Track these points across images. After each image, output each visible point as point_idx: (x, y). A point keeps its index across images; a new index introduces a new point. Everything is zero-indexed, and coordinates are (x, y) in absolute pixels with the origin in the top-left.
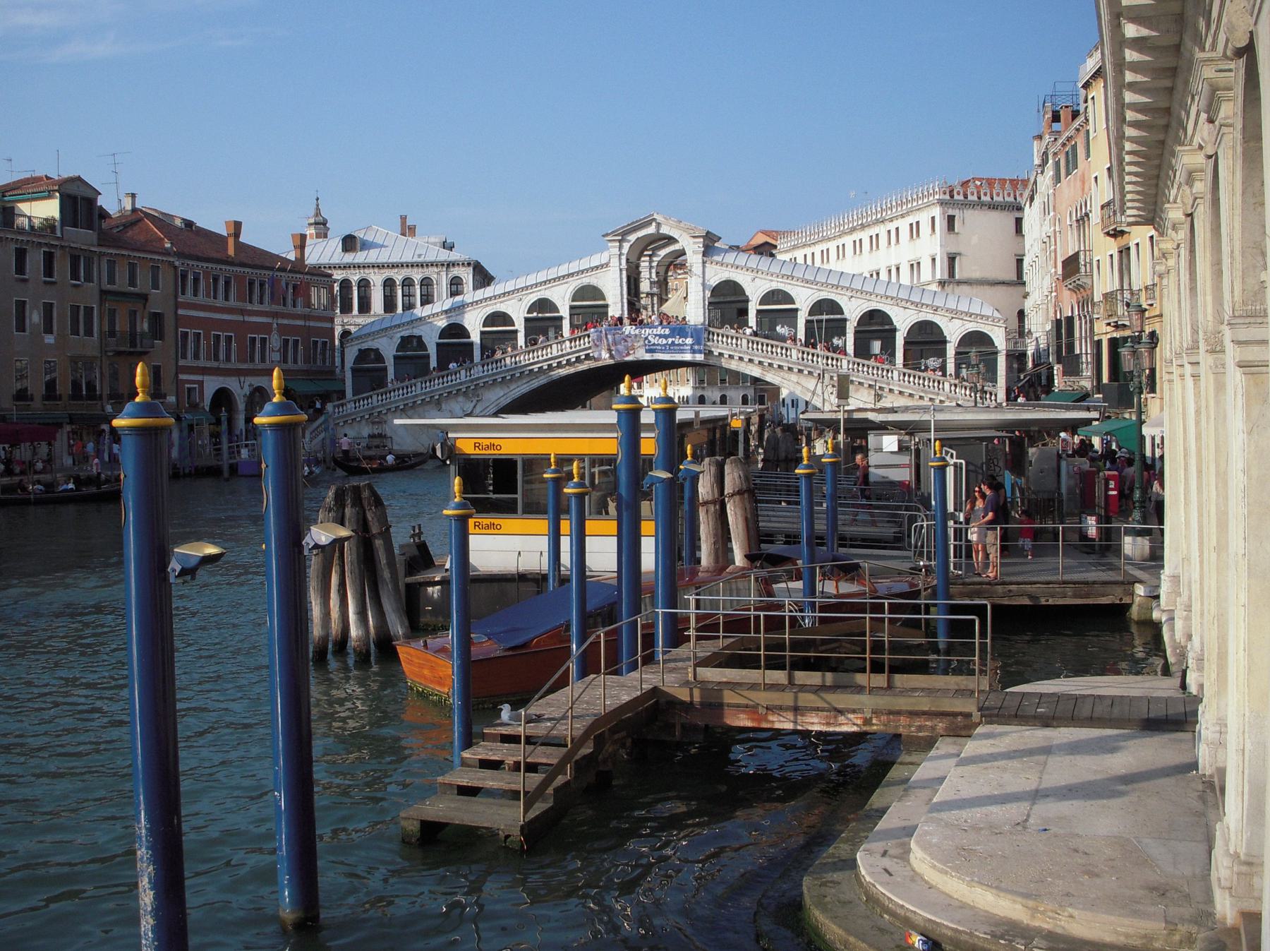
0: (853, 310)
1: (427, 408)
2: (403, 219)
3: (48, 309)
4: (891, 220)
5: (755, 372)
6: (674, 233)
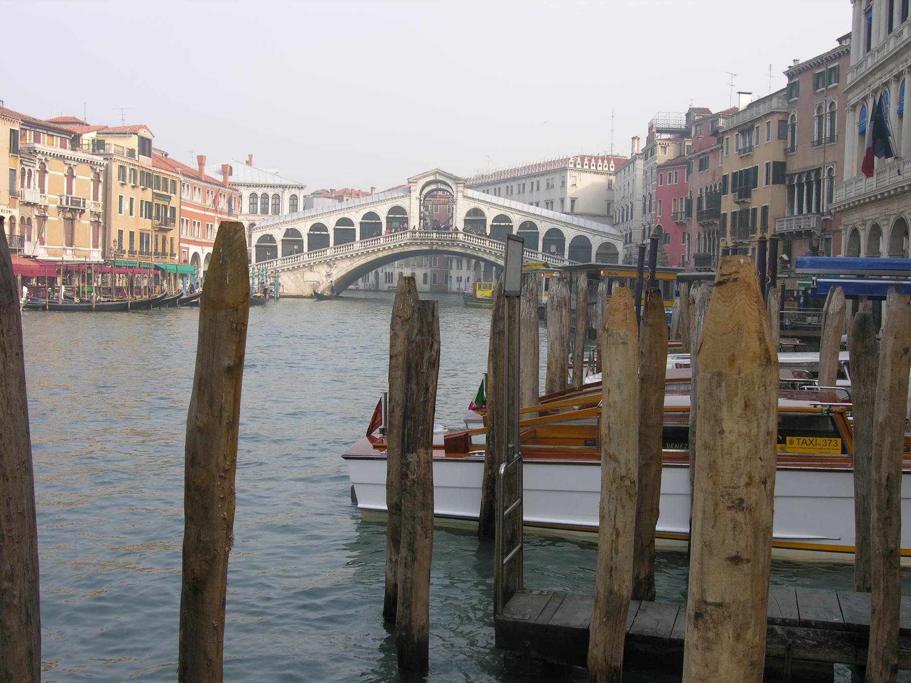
0: (543, 228)
2: (251, 156)
3: (132, 199)
4: (534, 176)
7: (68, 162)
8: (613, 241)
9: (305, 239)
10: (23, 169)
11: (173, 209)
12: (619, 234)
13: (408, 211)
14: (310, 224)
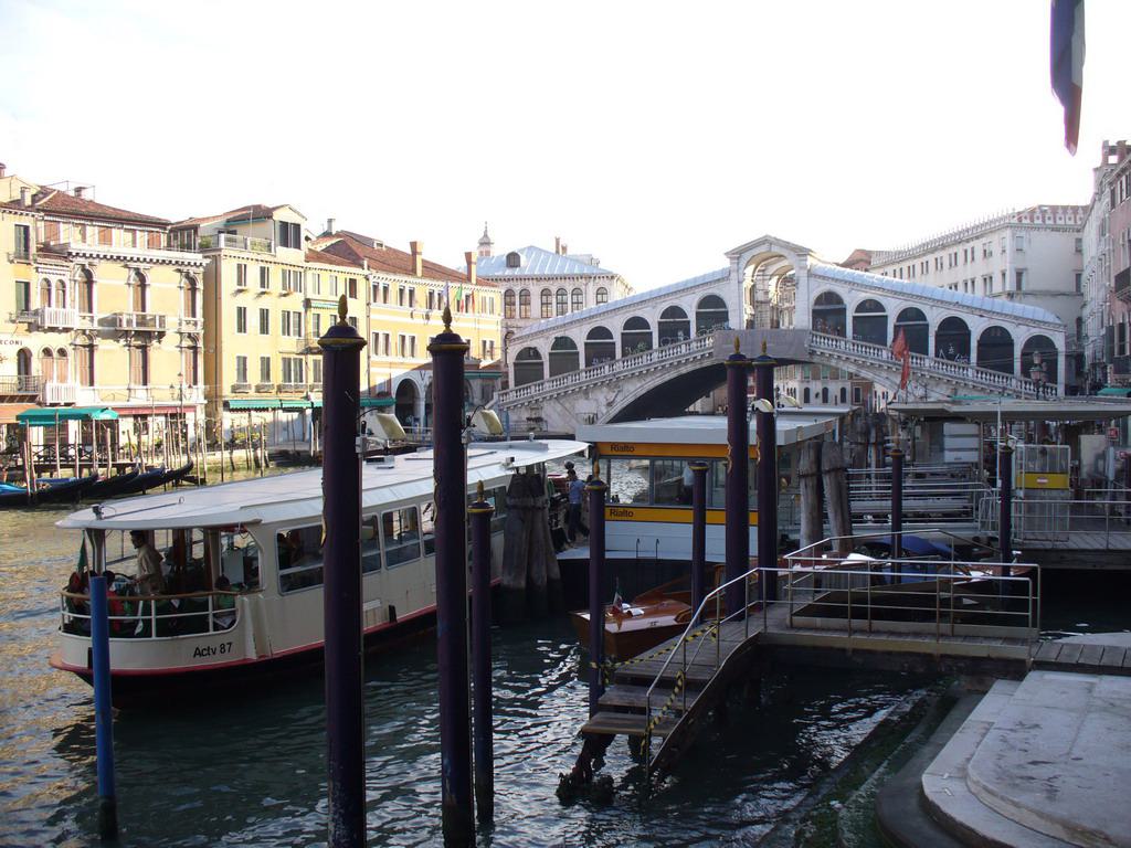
0: (934, 318)
2: (557, 241)
4: (968, 241)
5: (852, 369)
7: (134, 265)
8: (1047, 334)
9: (581, 349)
12: (1058, 321)
14: (587, 328)
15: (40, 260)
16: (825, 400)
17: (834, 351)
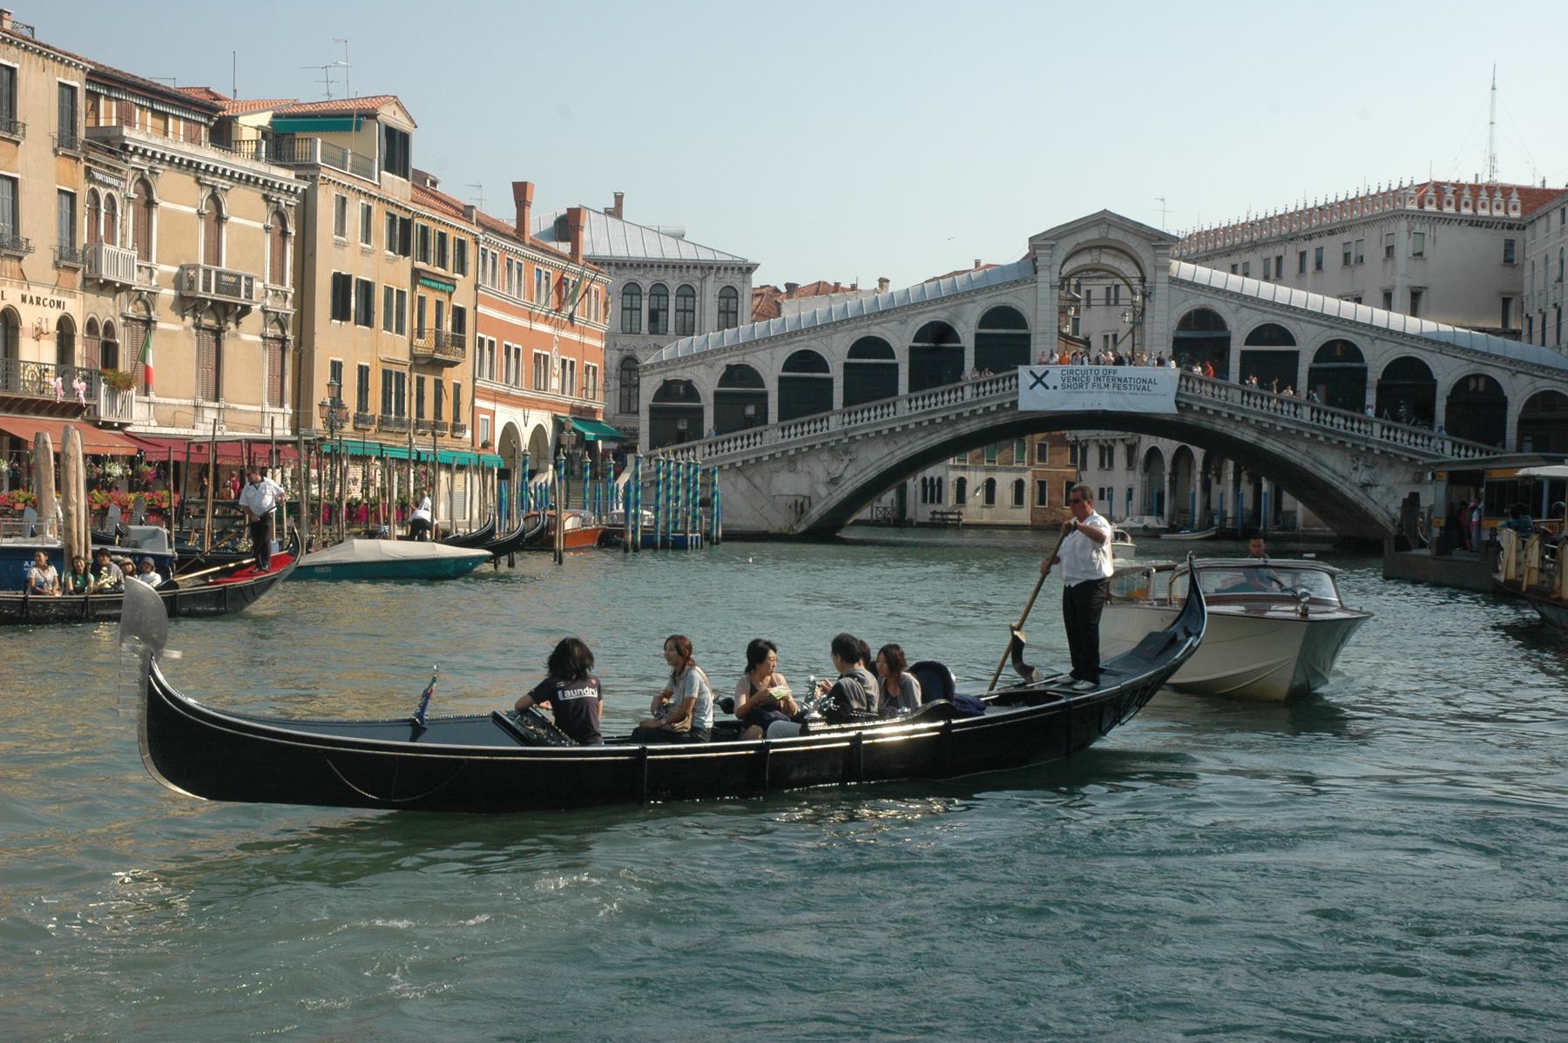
0: (1376, 360)
1: (772, 466)
2: (619, 199)
4: (1310, 238)
5: (1249, 436)
6: (1133, 243)
7: (209, 180)
9: (772, 387)
10: (94, 193)
11: (459, 314)
13: (1030, 321)
14: (784, 353)
15: (93, 156)
16: (990, 497)
17: (1224, 405)
